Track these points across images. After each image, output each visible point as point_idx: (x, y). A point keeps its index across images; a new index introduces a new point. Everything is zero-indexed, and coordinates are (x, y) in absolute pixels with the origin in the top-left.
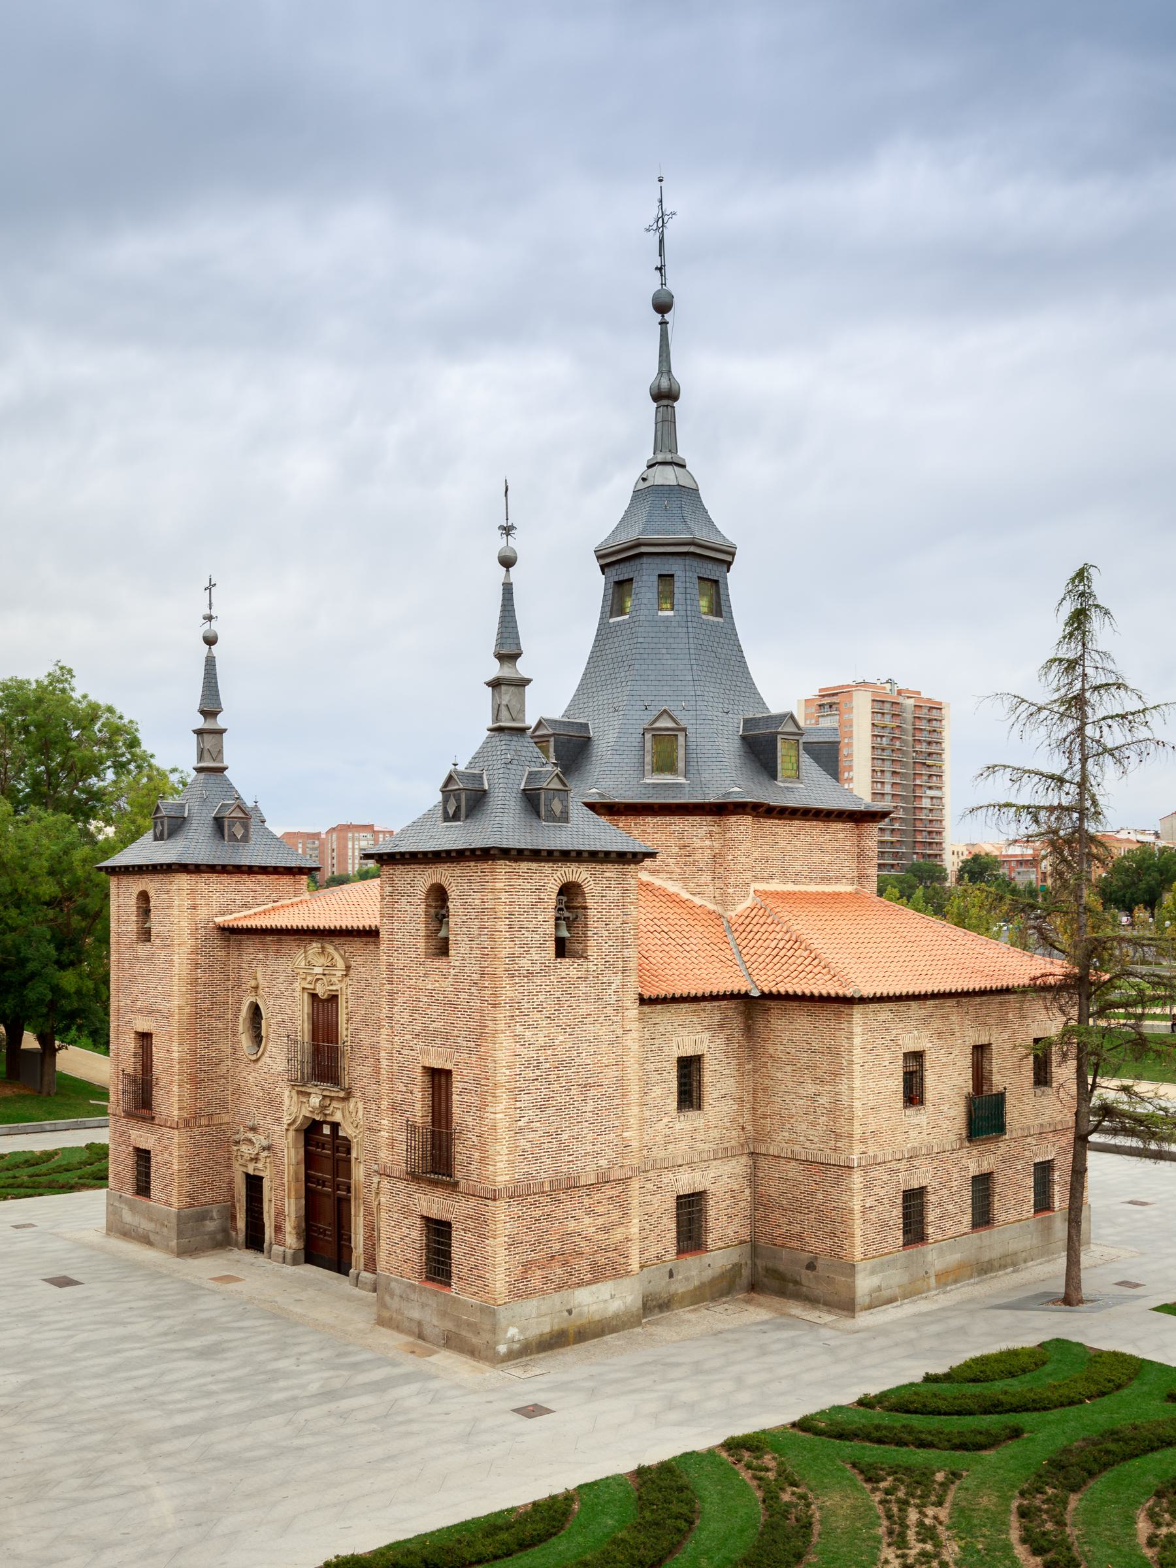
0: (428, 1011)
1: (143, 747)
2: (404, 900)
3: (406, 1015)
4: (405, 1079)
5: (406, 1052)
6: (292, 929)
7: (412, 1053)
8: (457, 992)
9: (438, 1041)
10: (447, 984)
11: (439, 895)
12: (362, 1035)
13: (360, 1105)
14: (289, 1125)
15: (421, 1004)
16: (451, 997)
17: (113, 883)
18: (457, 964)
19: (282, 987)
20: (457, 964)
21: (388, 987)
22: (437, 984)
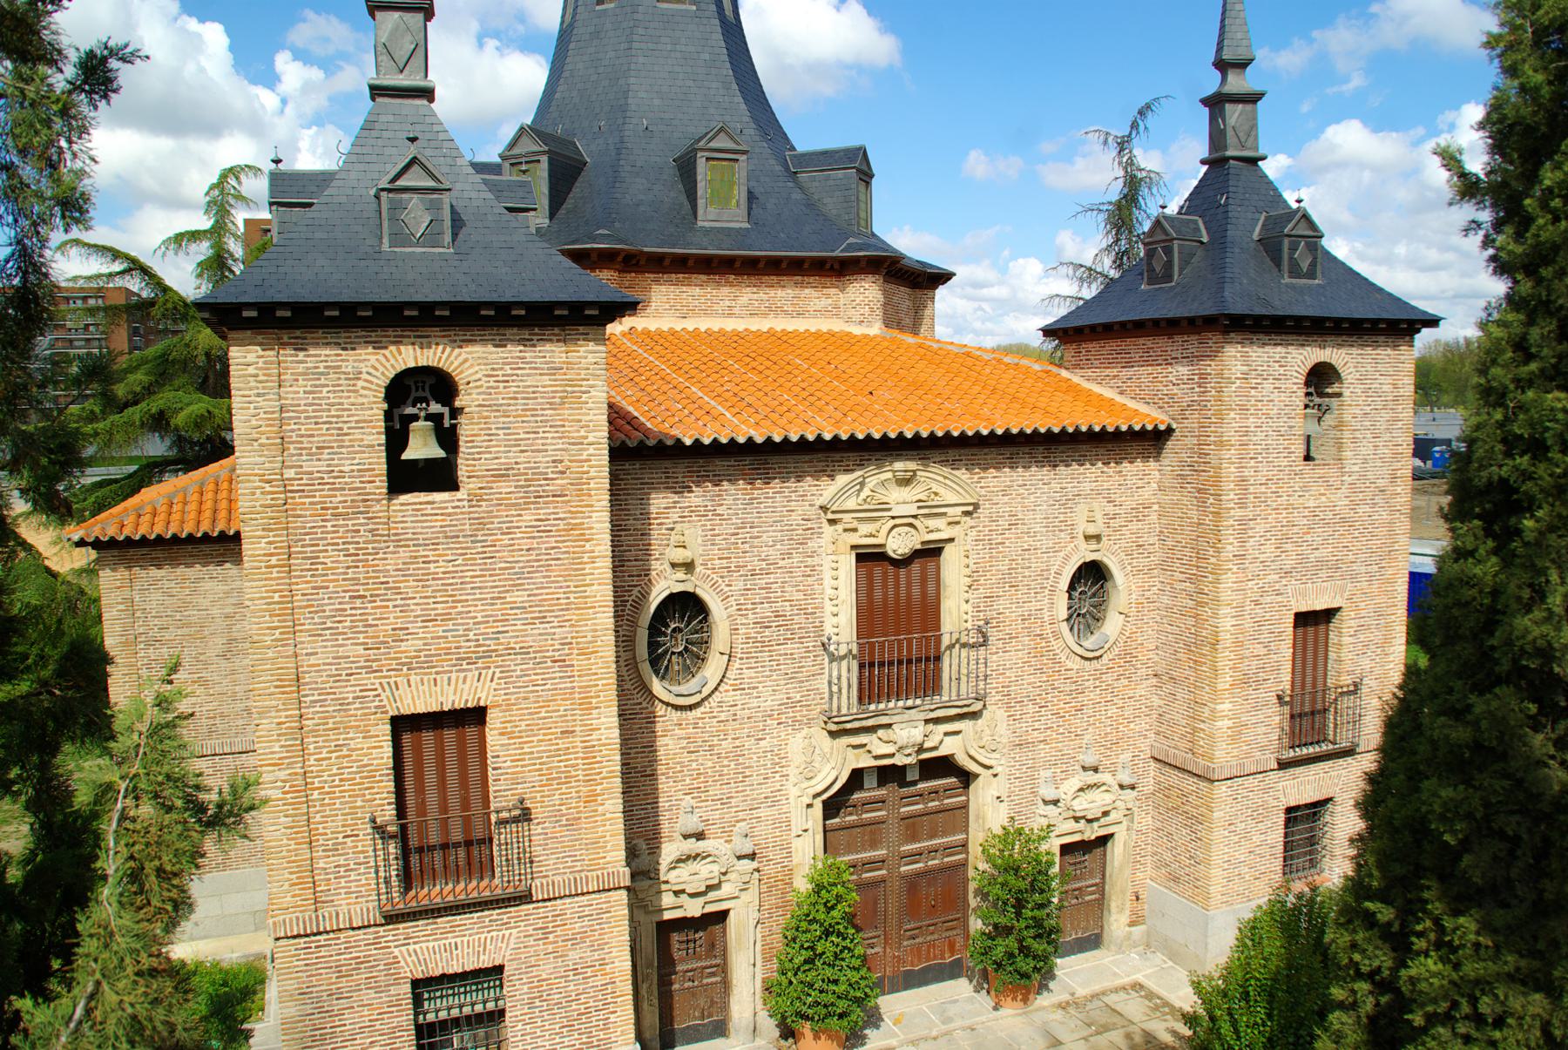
0: (1308, 537)
1: (1494, 79)
2: (1268, 386)
3: (1270, 548)
4: (1265, 637)
5: (1268, 599)
6: (1143, 431)
7: (1279, 599)
8: (1353, 506)
9: (1323, 574)
10: (1341, 500)
11: (1321, 379)
12: (1000, 605)
13: (1001, 714)
14: (816, 796)
15: (1296, 529)
16: (1347, 513)
17: (247, 361)
18: (1356, 468)
19: (773, 554)
20: (1356, 468)
21: (1238, 513)
22: (1323, 499)
